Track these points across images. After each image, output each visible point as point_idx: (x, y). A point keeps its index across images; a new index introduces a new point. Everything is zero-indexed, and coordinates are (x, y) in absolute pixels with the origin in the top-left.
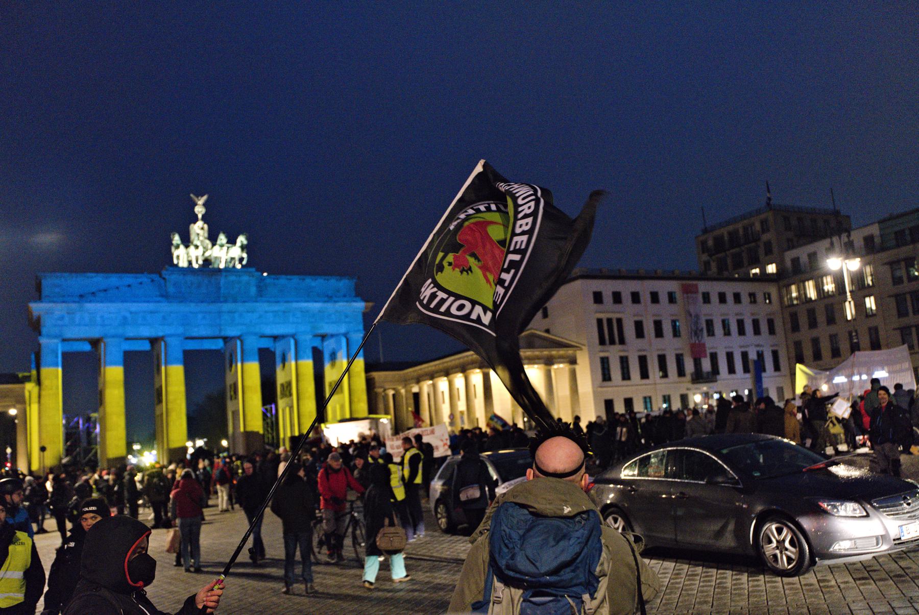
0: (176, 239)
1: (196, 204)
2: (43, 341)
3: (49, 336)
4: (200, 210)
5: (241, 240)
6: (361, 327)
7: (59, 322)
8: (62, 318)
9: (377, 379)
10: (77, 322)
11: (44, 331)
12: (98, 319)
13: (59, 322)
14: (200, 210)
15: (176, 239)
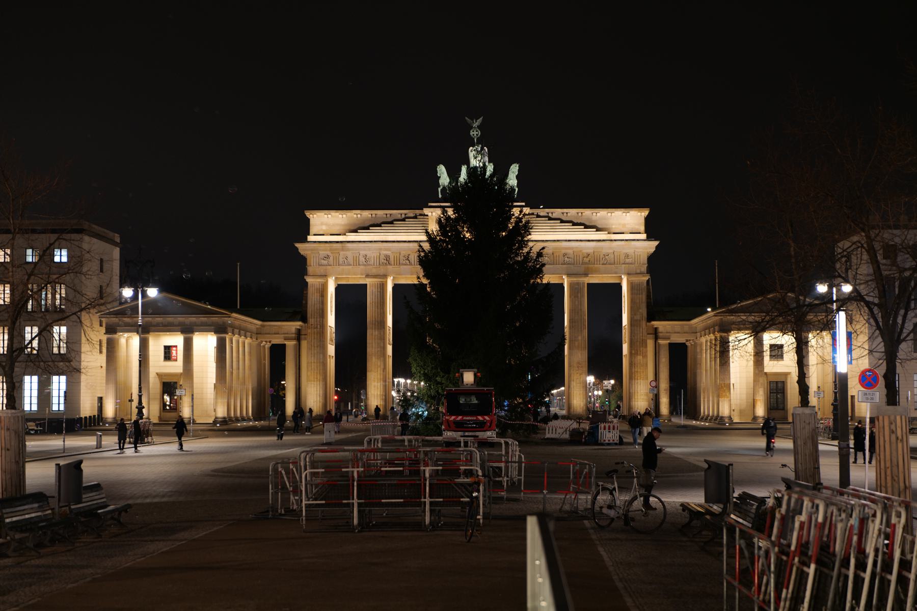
0: (442, 170)
1: (472, 128)
2: (309, 280)
3: (314, 276)
4: (475, 133)
5: (514, 169)
6: (644, 268)
7: (325, 262)
8: (328, 257)
9: (661, 329)
10: (341, 260)
11: (310, 270)
12: (362, 259)
13: (325, 262)
14: (475, 133)
15: (442, 170)
